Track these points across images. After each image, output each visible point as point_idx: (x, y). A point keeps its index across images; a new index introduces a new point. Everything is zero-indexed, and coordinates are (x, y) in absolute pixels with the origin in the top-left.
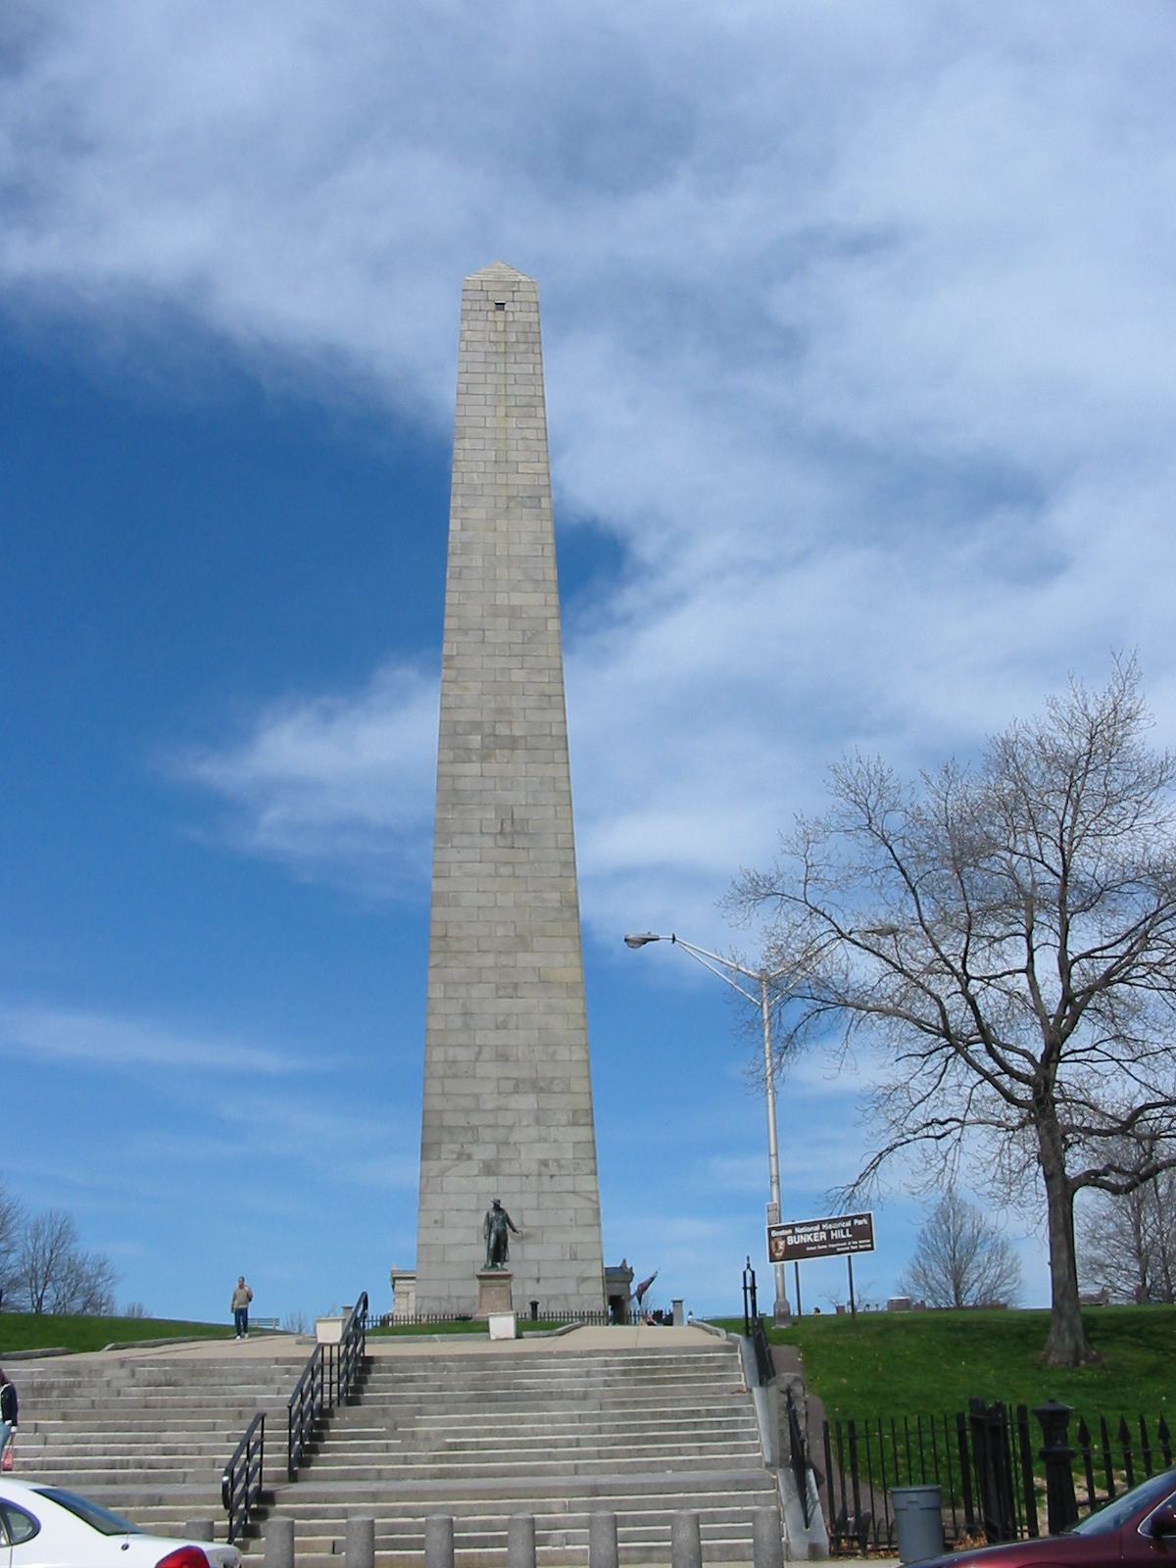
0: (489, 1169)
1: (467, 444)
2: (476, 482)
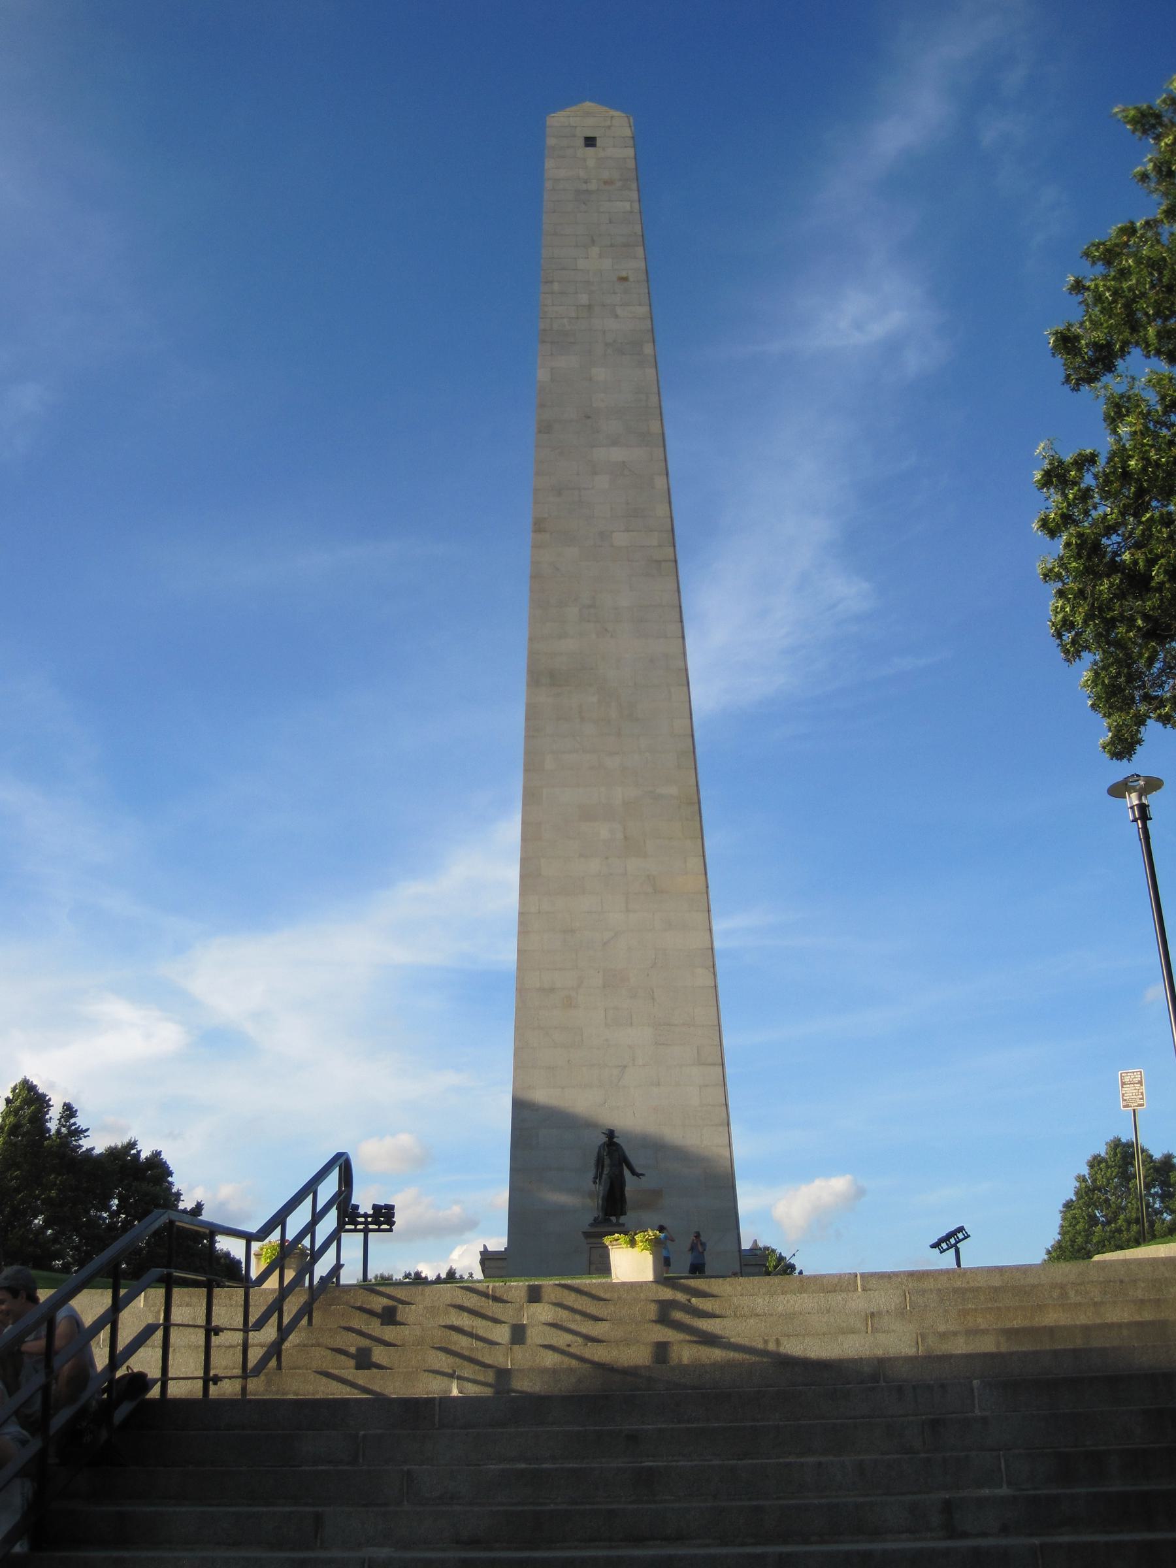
1: (556, 287)
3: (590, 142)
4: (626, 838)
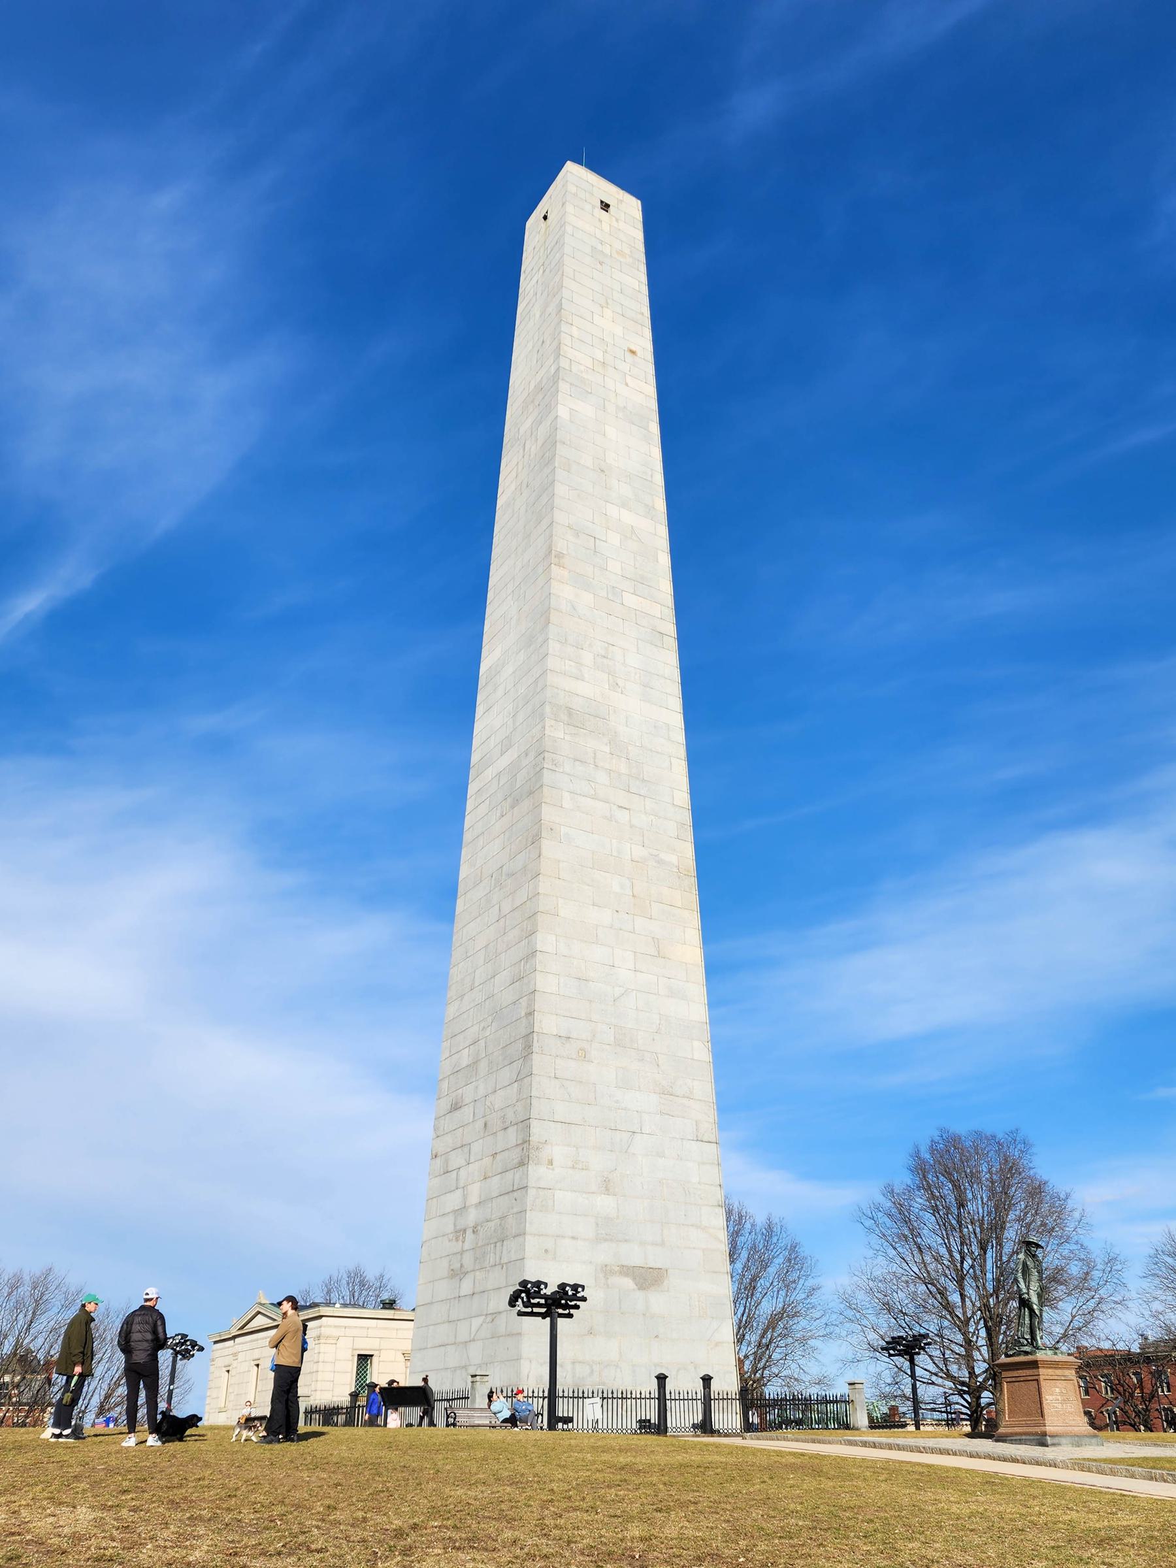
3: (605, 206)
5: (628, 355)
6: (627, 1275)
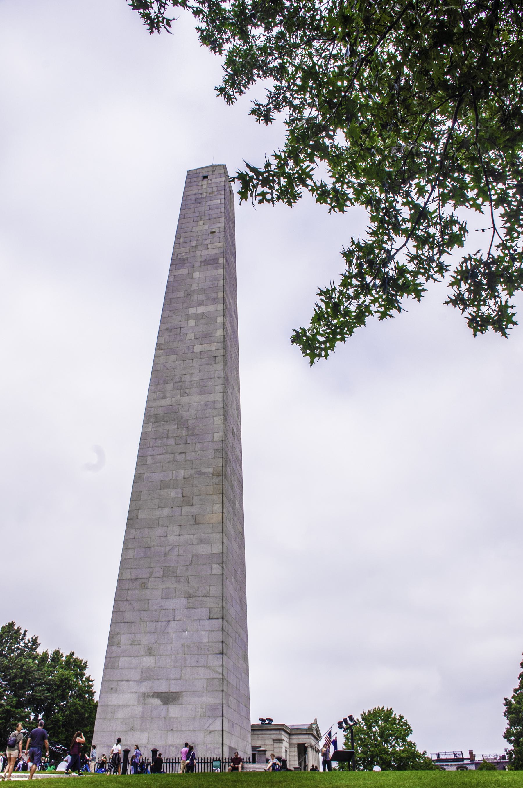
0: (150, 652)
2: (184, 257)
3: (205, 177)
4: (183, 496)
5: (211, 236)
6: (157, 697)
